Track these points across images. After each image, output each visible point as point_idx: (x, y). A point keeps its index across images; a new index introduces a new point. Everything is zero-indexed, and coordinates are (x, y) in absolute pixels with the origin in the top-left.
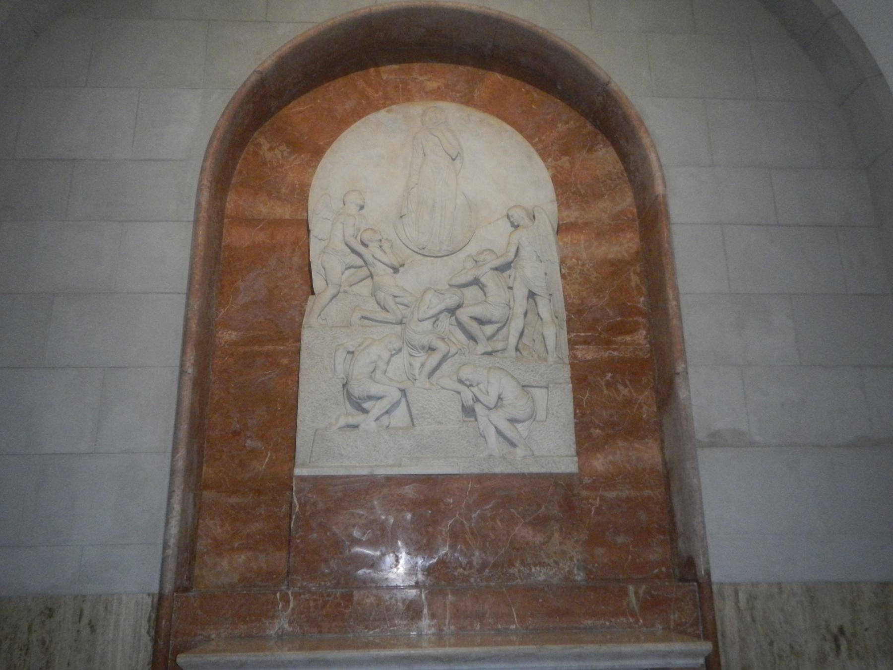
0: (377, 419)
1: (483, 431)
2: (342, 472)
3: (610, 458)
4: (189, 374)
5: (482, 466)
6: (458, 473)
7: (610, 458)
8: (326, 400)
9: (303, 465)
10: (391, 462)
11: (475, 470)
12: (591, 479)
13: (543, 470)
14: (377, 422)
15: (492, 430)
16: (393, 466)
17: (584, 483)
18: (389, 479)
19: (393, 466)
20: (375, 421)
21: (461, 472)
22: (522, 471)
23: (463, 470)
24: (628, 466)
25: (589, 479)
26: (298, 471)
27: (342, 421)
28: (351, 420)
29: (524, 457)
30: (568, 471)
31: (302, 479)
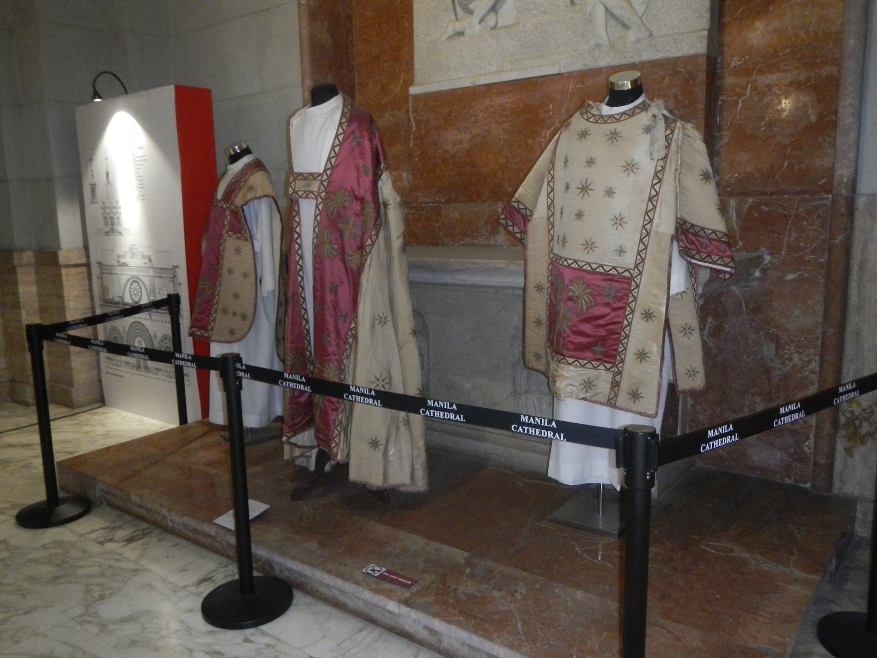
0: (482, 20)
1: (590, 14)
2: (447, 86)
3: (776, 24)
4: (303, 5)
5: (585, 60)
6: (558, 72)
7: (776, 24)
8: (437, 7)
9: (420, 84)
10: (495, 68)
11: (577, 67)
12: (742, 60)
13: (659, 56)
14: (483, 24)
15: (601, 12)
16: (495, 73)
17: (732, 66)
18: (490, 87)
19: (495, 73)
20: (480, 23)
21: (562, 71)
22: (632, 61)
23: (565, 68)
24: (802, 34)
25: (740, 61)
26: (414, 90)
27: (450, 32)
28: (458, 27)
29: (638, 41)
30: (692, 52)
31: (417, 98)
